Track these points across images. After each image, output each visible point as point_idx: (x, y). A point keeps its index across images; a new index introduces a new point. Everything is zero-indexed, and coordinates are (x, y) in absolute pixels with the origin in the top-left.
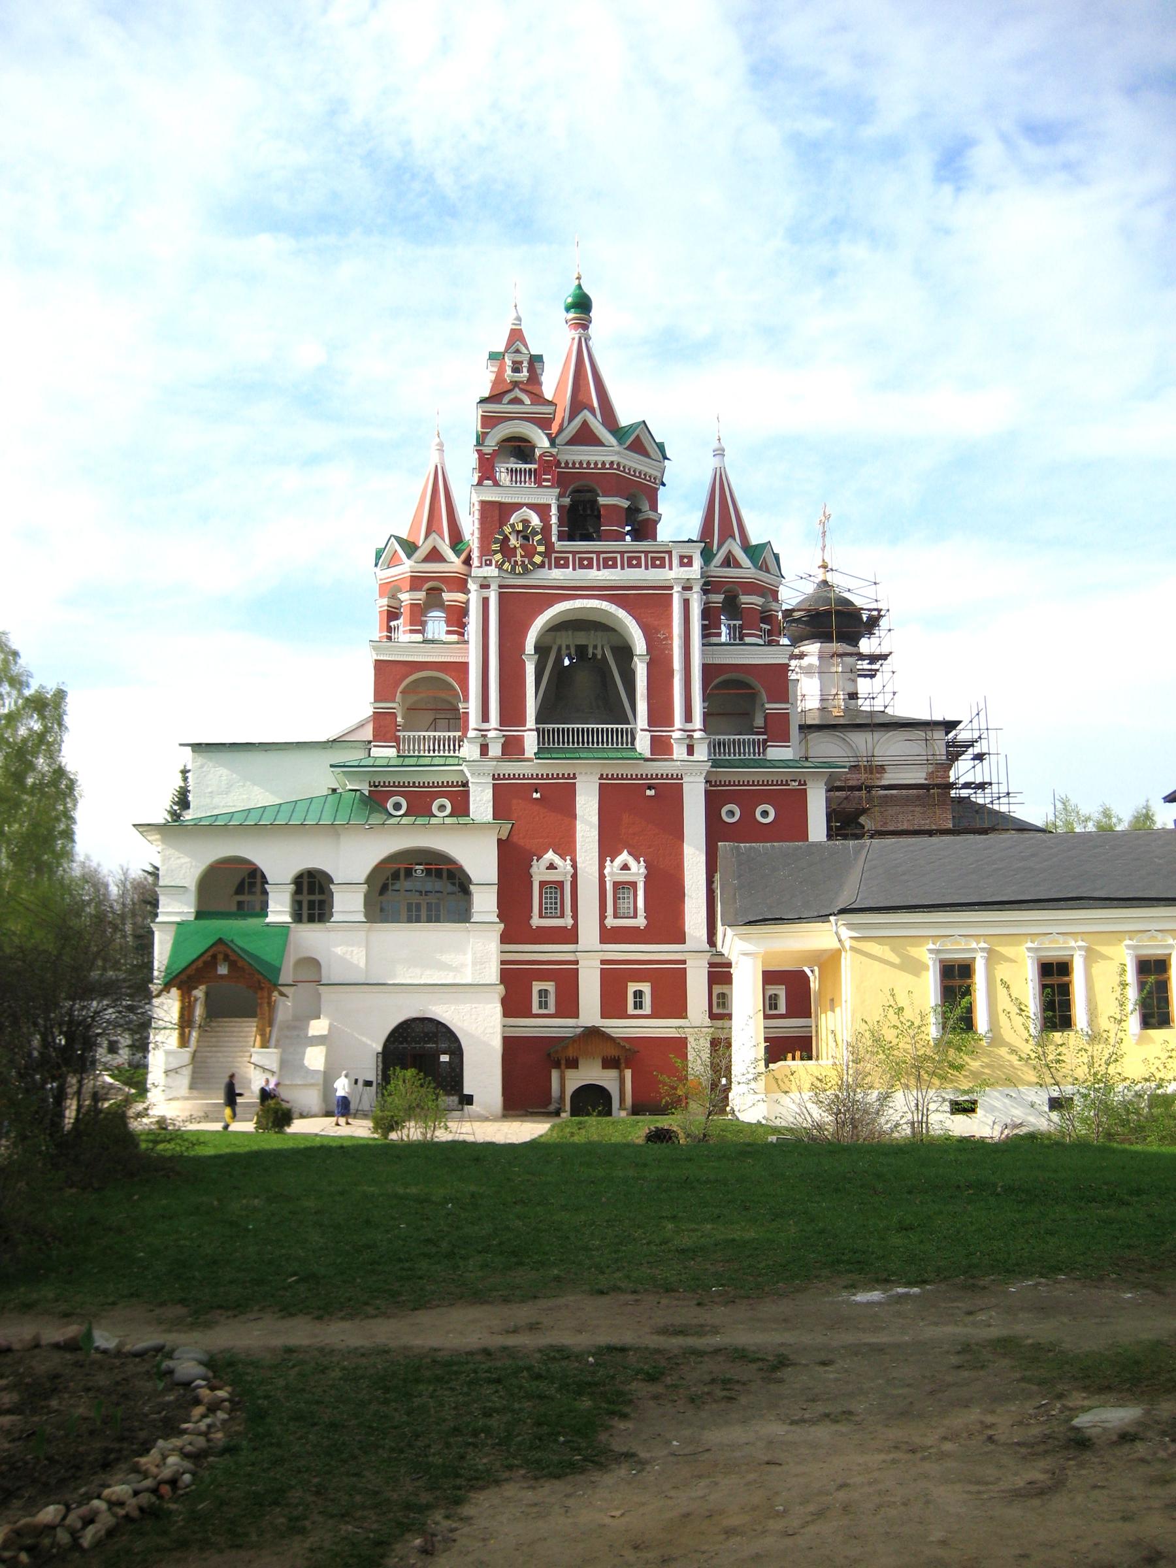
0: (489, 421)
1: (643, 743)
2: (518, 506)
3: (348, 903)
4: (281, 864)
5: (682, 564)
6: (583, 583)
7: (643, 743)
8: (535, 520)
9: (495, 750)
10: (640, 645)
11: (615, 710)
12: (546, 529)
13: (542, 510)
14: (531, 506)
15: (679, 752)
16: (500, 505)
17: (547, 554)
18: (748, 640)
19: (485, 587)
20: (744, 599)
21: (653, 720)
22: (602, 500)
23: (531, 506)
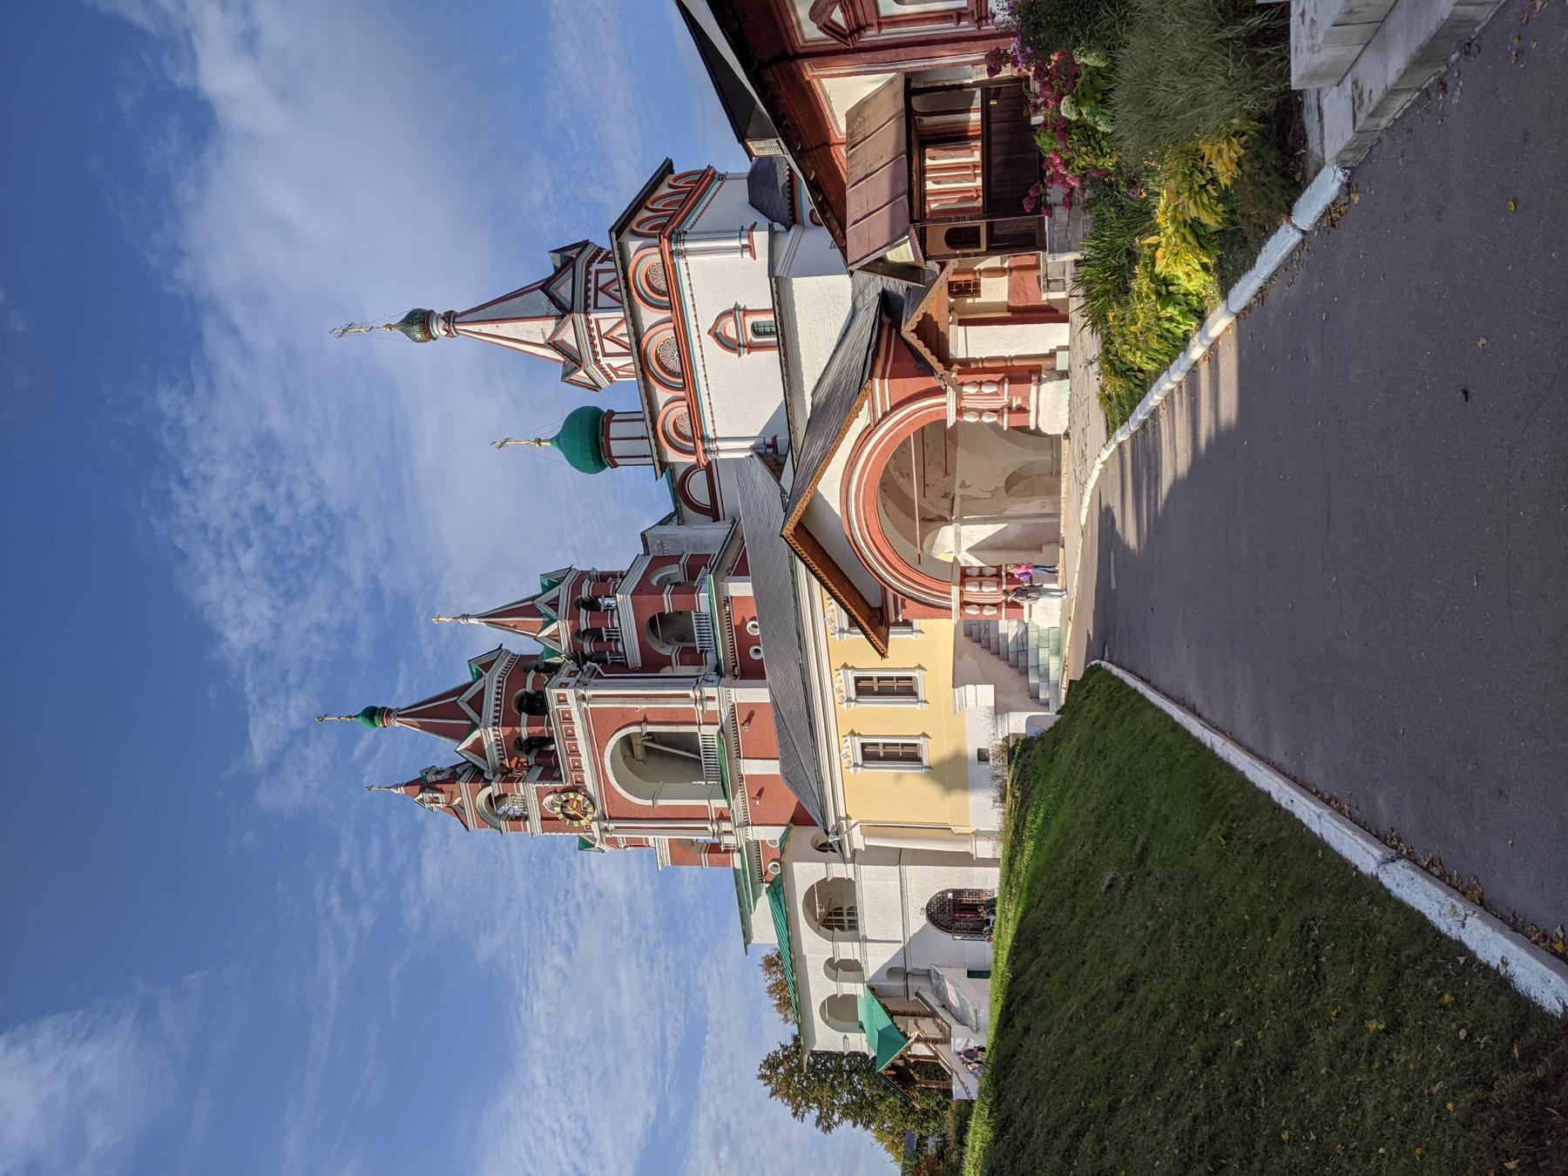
1: (712, 730)
2: (541, 808)
3: (848, 950)
5: (565, 701)
6: (591, 760)
9: (726, 826)
11: (688, 743)
14: (540, 802)
15: (711, 706)
16: (543, 819)
17: (575, 790)
18: (616, 624)
19: (606, 830)
20: (583, 628)
21: (694, 723)
22: (524, 736)
23: (540, 799)
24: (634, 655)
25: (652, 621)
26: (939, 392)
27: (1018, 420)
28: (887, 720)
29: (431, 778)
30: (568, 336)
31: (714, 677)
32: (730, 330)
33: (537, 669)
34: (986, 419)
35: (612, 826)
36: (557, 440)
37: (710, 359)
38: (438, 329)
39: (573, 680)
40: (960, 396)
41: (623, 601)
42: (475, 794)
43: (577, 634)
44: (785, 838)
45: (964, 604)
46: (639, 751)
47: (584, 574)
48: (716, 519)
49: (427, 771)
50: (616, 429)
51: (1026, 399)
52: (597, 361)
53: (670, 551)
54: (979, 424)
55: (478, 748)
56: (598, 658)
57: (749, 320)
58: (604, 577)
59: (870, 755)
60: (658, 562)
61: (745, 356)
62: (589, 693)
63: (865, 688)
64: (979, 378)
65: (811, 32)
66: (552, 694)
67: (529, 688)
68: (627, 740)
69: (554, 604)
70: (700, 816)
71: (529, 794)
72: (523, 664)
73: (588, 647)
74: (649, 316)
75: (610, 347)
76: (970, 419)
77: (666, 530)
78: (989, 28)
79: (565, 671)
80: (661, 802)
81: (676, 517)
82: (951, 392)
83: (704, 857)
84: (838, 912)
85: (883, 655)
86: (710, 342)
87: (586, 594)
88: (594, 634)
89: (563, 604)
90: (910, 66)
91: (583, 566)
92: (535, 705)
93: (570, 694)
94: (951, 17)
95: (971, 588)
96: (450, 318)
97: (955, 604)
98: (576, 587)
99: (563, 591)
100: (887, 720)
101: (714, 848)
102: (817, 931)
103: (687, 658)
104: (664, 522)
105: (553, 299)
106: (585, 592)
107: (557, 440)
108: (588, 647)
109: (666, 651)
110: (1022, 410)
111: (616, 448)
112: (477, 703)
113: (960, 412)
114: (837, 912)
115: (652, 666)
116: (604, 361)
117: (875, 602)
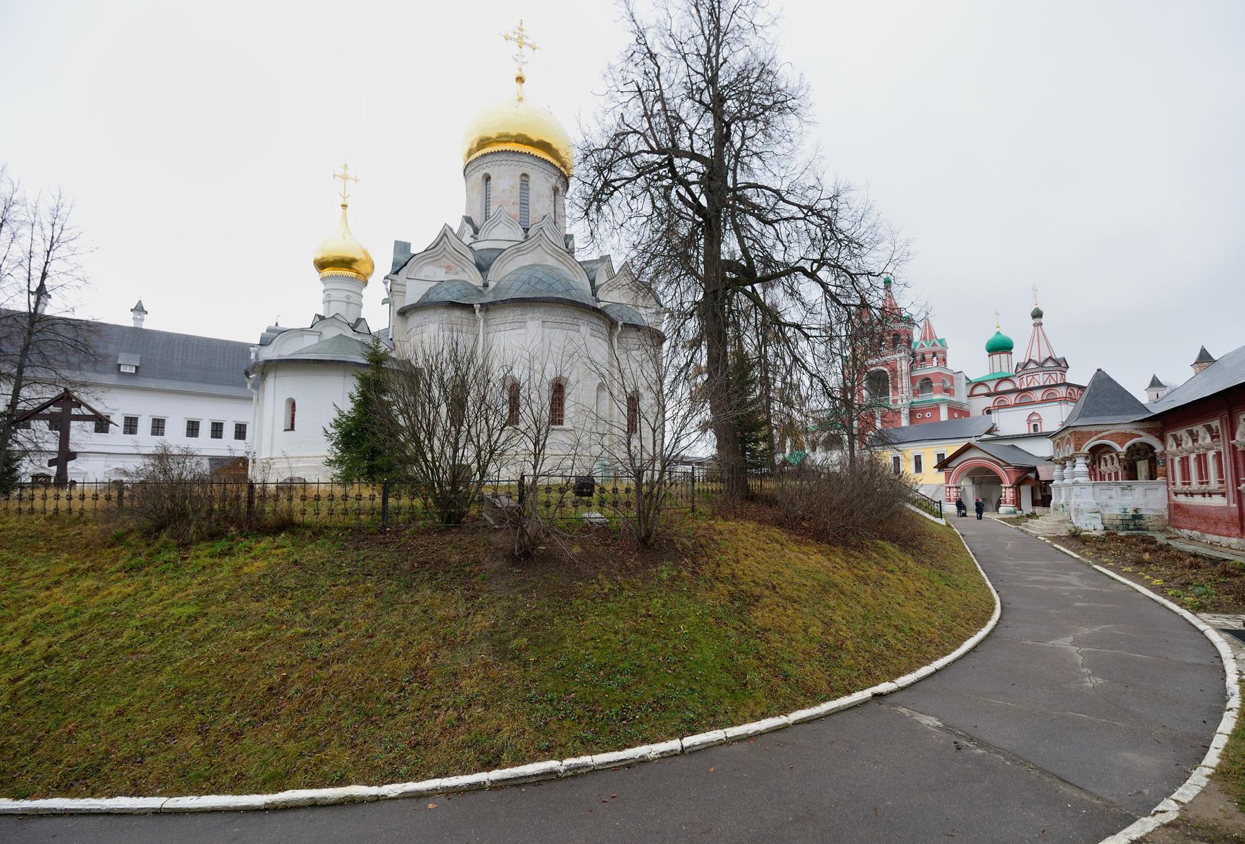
24: (915, 374)
30: (1032, 366)
37: (1026, 412)
38: (1037, 320)
41: (937, 370)
43: (923, 355)
47: (945, 353)
50: (1004, 356)
58: (944, 360)
60: (951, 378)
69: (934, 345)
72: (909, 334)
73: (918, 358)
74: (1038, 395)
88: (923, 359)
89: (934, 349)
98: (940, 352)
105: (1046, 360)
108: (918, 358)
111: (996, 357)
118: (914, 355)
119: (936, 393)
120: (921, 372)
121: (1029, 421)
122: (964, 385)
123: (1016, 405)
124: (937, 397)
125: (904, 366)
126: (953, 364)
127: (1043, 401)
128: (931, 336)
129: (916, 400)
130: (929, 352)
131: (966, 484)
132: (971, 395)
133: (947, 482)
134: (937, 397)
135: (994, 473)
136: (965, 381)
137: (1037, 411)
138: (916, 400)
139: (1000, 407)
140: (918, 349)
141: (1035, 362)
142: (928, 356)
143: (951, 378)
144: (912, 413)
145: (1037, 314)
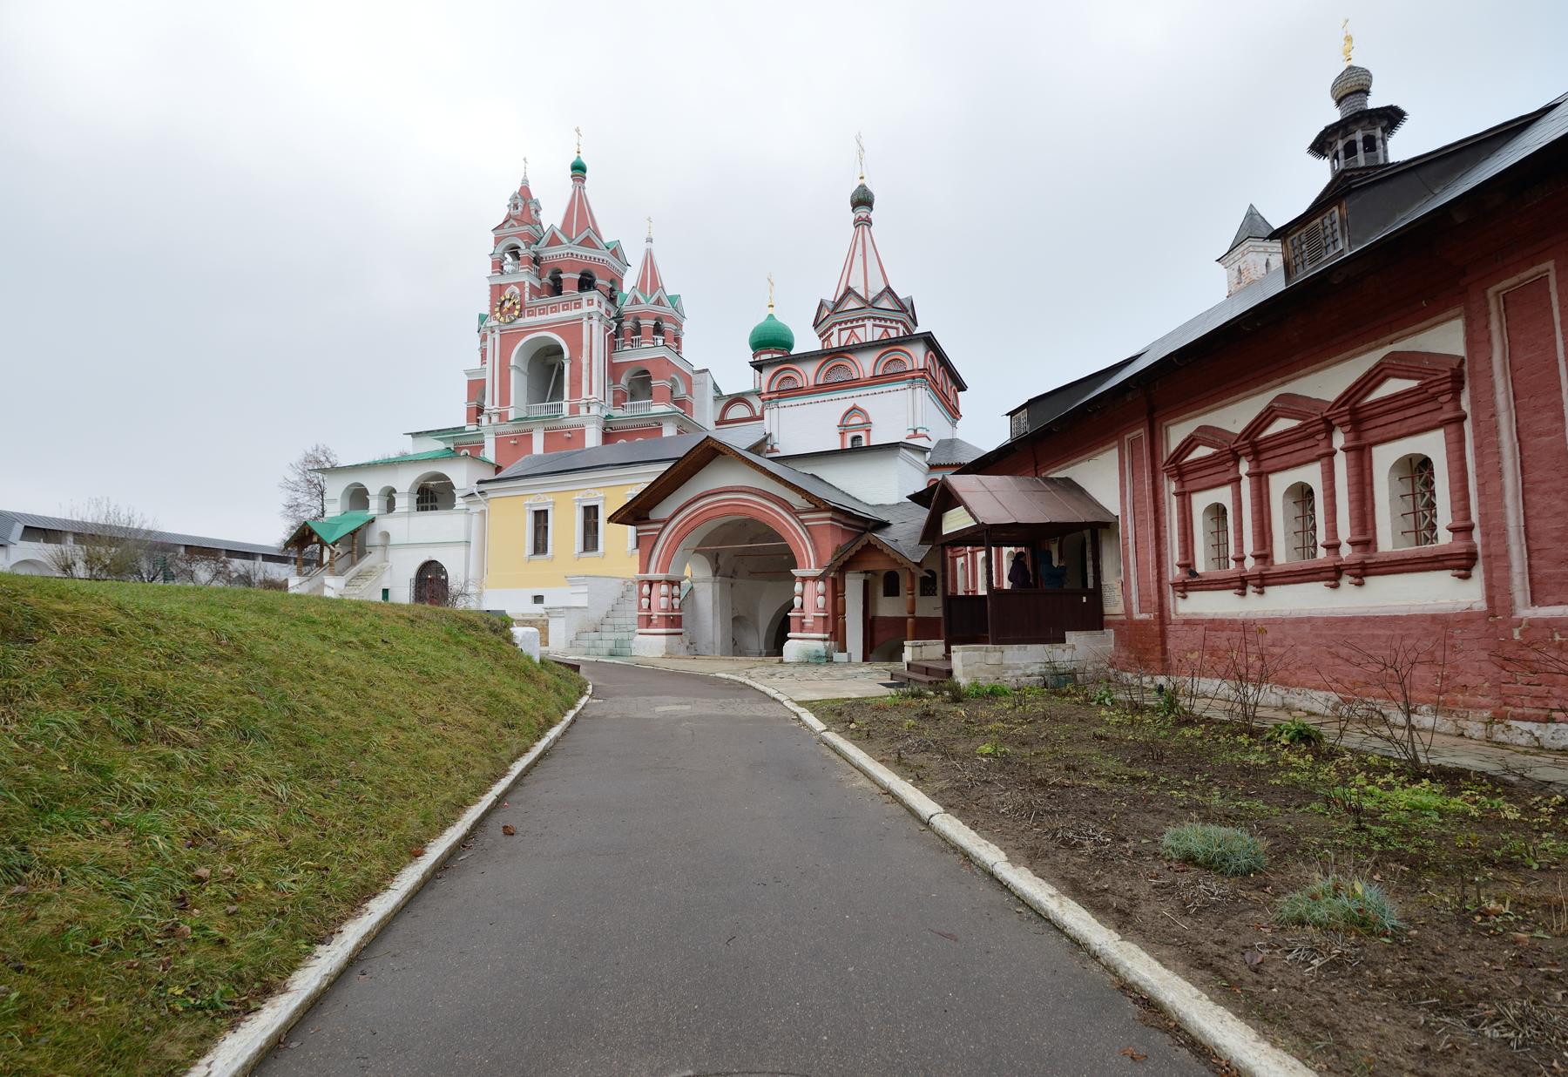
0: (498, 240)
1: (566, 407)
4: (374, 485)
6: (545, 322)
7: (566, 407)
8: (517, 291)
10: (567, 354)
12: (522, 295)
13: (520, 285)
15: (583, 411)
21: (571, 396)
25: (646, 372)
26: (818, 566)
27: (794, 624)
28: (566, 529)
29: (532, 207)
31: (604, 413)
32: (856, 420)
33: (612, 290)
34: (797, 601)
35: (497, 337)
36: (771, 316)
38: (862, 212)
39: (603, 311)
40: (815, 579)
41: (661, 353)
42: (520, 236)
44: (484, 461)
45: (651, 584)
46: (551, 360)
48: (717, 423)
49: (537, 203)
51: (812, 630)
52: (834, 325)
53: (695, 389)
54: (793, 594)
55: (554, 241)
56: (622, 330)
57: (863, 434)
58: (677, 340)
59: (541, 517)
61: (837, 431)
62: (595, 323)
63: (591, 513)
64: (830, 594)
65: (1177, 434)
66: (594, 295)
67: (598, 281)
68: (560, 351)
69: (658, 302)
70: (505, 400)
71: (522, 277)
72: (616, 282)
74: (866, 364)
75: (845, 334)
76: (798, 587)
77: (710, 386)
78: (1170, 594)
79: (610, 307)
80: (513, 373)
81: (719, 396)
82: (819, 572)
83: (474, 404)
84: (434, 499)
85: (610, 519)
86: (848, 405)
87: (665, 328)
88: (637, 330)
89: (659, 310)
90: (1128, 529)
91: (685, 324)
92: (586, 283)
93: (595, 308)
94: (1364, 531)
95: (664, 589)
96: (868, 222)
97: (652, 574)
98: (670, 319)
99: (667, 310)
100: (566, 529)
101: (480, 411)
102: (416, 482)
103: (619, 396)
104: (716, 387)
106: (667, 326)
107: (771, 316)
108: (628, 325)
109: (624, 381)
110: (802, 627)
112: (587, 242)
113: (804, 579)
114: (432, 496)
115: (614, 371)
116: (835, 330)
117: (653, 515)
118: (619, 318)
119: (660, 400)
120: (630, 355)
121: (844, 427)
122: (710, 401)
123: (819, 389)
124: (659, 408)
125: (595, 337)
126: (695, 351)
127: (876, 380)
128: (656, 285)
129: (618, 413)
130: (647, 315)
131: (696, 574)
132: (721, 422)
133: (645, 567)
134: (659, 408)
135: (773, 535)
136: (711, 393)
137: (861, 403)
138: (618, 413)
139: (783, 394)
140: (627, 307)
141: (858, 296)
142: (647, 323)
143: (688, 380)
144: (608, 437)
145: (863, 200)
